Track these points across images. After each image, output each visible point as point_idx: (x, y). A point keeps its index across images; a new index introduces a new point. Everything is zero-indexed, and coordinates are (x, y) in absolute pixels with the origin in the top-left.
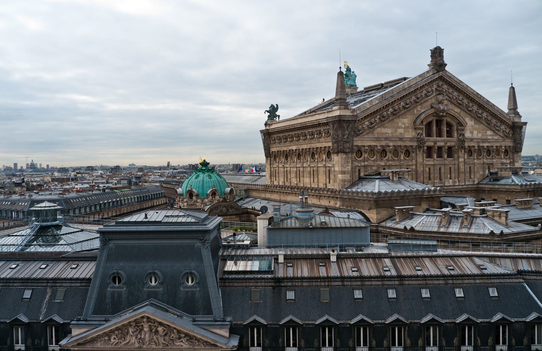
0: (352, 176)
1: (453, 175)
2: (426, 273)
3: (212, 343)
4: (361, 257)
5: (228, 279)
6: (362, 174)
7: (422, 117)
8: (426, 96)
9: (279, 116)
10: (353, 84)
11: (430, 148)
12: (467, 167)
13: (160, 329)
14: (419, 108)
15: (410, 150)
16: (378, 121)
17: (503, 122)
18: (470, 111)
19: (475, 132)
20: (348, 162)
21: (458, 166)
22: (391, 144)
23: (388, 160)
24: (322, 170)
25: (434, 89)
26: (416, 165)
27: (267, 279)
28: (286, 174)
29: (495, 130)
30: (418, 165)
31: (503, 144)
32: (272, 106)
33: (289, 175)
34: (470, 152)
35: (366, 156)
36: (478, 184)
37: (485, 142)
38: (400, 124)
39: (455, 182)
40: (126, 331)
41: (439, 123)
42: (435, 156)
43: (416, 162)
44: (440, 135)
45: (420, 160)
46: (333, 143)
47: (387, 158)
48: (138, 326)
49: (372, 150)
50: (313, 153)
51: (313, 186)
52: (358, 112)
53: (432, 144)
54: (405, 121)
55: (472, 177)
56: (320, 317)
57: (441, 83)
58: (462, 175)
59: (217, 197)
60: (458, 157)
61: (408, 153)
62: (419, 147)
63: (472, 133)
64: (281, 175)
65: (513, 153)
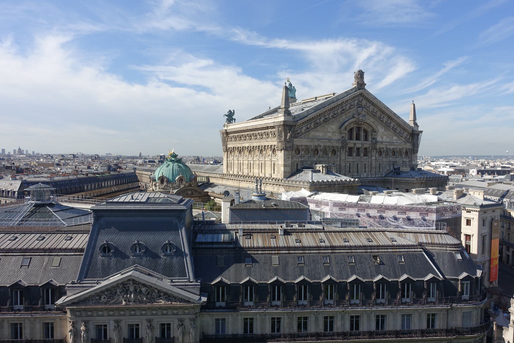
0: (292, 169)
1: (367, 169)
2: (351, 244)
3: (186, 299)
4: (302, 232)
5: (199, 248)
6: (299, 167)
8: (350, 108)
9: (235, 119)
10: (293, 96)
11: (350, 149)
12: (378, 163)
13: (143, 289)
14: (344, 117)
15: (336, 150)
16: (312, 127)
17: (405, 130)
18: (382, 121)
19: (385, 137)
20: (289, 158)
21: (371, 163)
22: (322, 144)
23: (319, 157)
24: (268, 163)
25: (356, 103)
26: (340, 161)
27: (230, 248)
28: (240, 165)
29: (399, 135)
30: (342, 162)
32: (230, 111)
33: (242, 167)
34: (380, 153)
35: (303, 153)
36: (385, 176)
37: (391, 145)
38: (329, 129)
39: (368, 175)
40: (115, 291)
41: (359, 129)
42: (354, 154)
43: (340, 159)
44: (358, 138)
45: (343, 157)
46: (278, 143)
47: (318, 155)
48: (125, 287)
49: (307, 149)
50: (261, 150)
51: (260, 176)
52: (298, 119)
53: (352, 146)
54: (333, 127)
55: (381, 171)
56: (271, 278)
57: (361, 99)
58: (374, 170)
59: (184, 182)
60: (371, 156)
61: (334, 152)
62: (343, 147)
63: (382, 138)
64: (236, 166)
65: (411, 154)
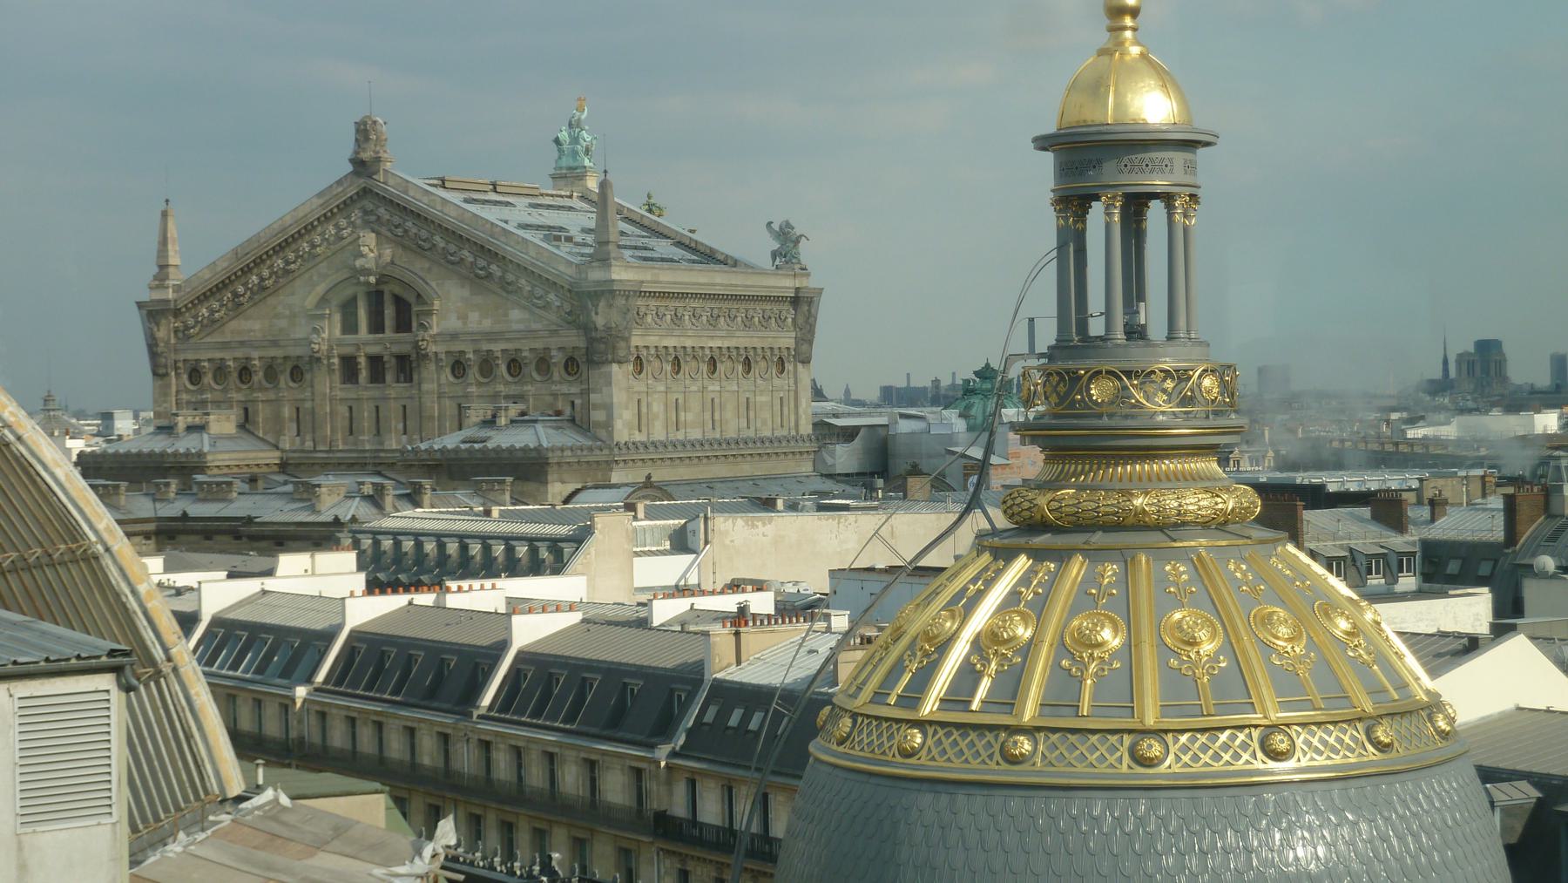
7: (321, 289)
22: (255, 354)
31: (554, 343)
37: (496, 340)
38: (280, 309)
63: (463, 317)
